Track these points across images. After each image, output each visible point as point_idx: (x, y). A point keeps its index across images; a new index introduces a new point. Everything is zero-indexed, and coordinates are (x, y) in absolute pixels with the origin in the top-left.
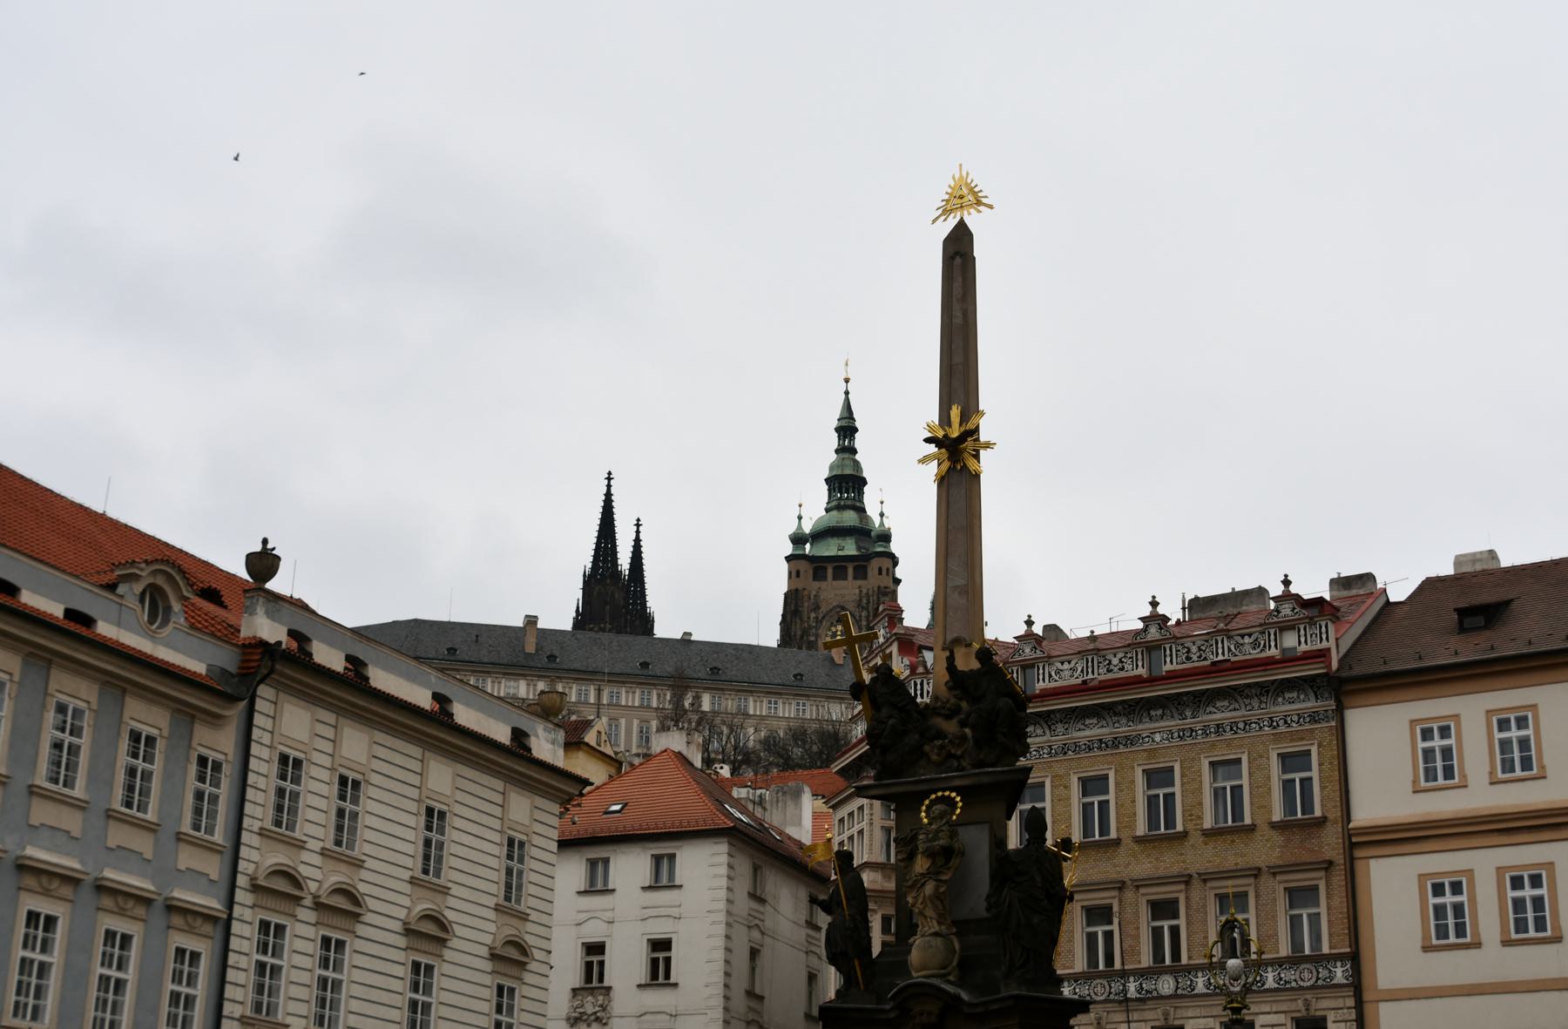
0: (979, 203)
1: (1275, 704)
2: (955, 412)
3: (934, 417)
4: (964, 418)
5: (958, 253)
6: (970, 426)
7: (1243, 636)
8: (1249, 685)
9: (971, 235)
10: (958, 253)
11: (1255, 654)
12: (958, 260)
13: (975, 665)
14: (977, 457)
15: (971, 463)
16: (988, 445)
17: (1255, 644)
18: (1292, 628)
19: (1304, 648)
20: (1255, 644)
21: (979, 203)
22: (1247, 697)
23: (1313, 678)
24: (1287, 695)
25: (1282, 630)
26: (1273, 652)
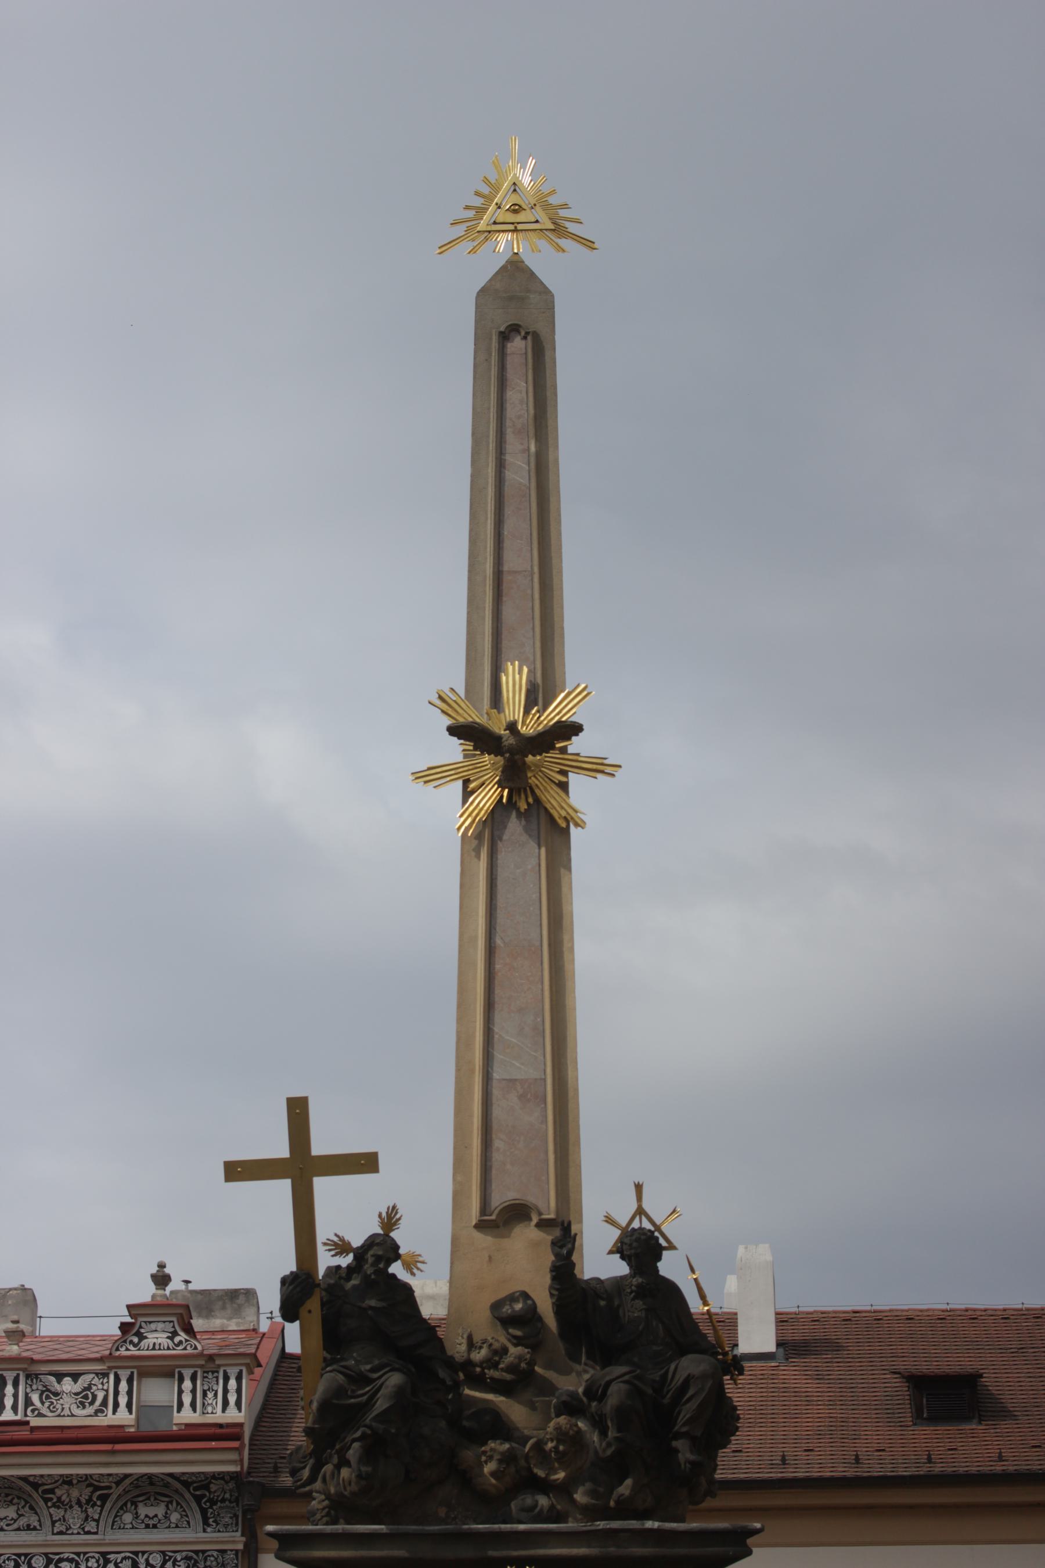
0: (559, 229)
1: (116, 1524)
2: (515, 680)
3: (455, 680)
4: (538, 695)
5: (515, 330)
6: (553, 714)
7: (59, 1377)
8: (67, 1481)
9: (546, 292)
10: (515, 330)
11: (83, 1417)
12: (517, 345)
13: (619, 1268)
14: (564, 787)
15: (551, 797)
16: (598, 768)
17: (85, 1397)
18: (170, 1375)
19: (187, 1416)
20: (85, 1397)
21: (559, 229)
22: (59, 1504)
23: (205, 1482)
24: (143, 1510)
25: (145, 1373)
26: (123, 1417)
